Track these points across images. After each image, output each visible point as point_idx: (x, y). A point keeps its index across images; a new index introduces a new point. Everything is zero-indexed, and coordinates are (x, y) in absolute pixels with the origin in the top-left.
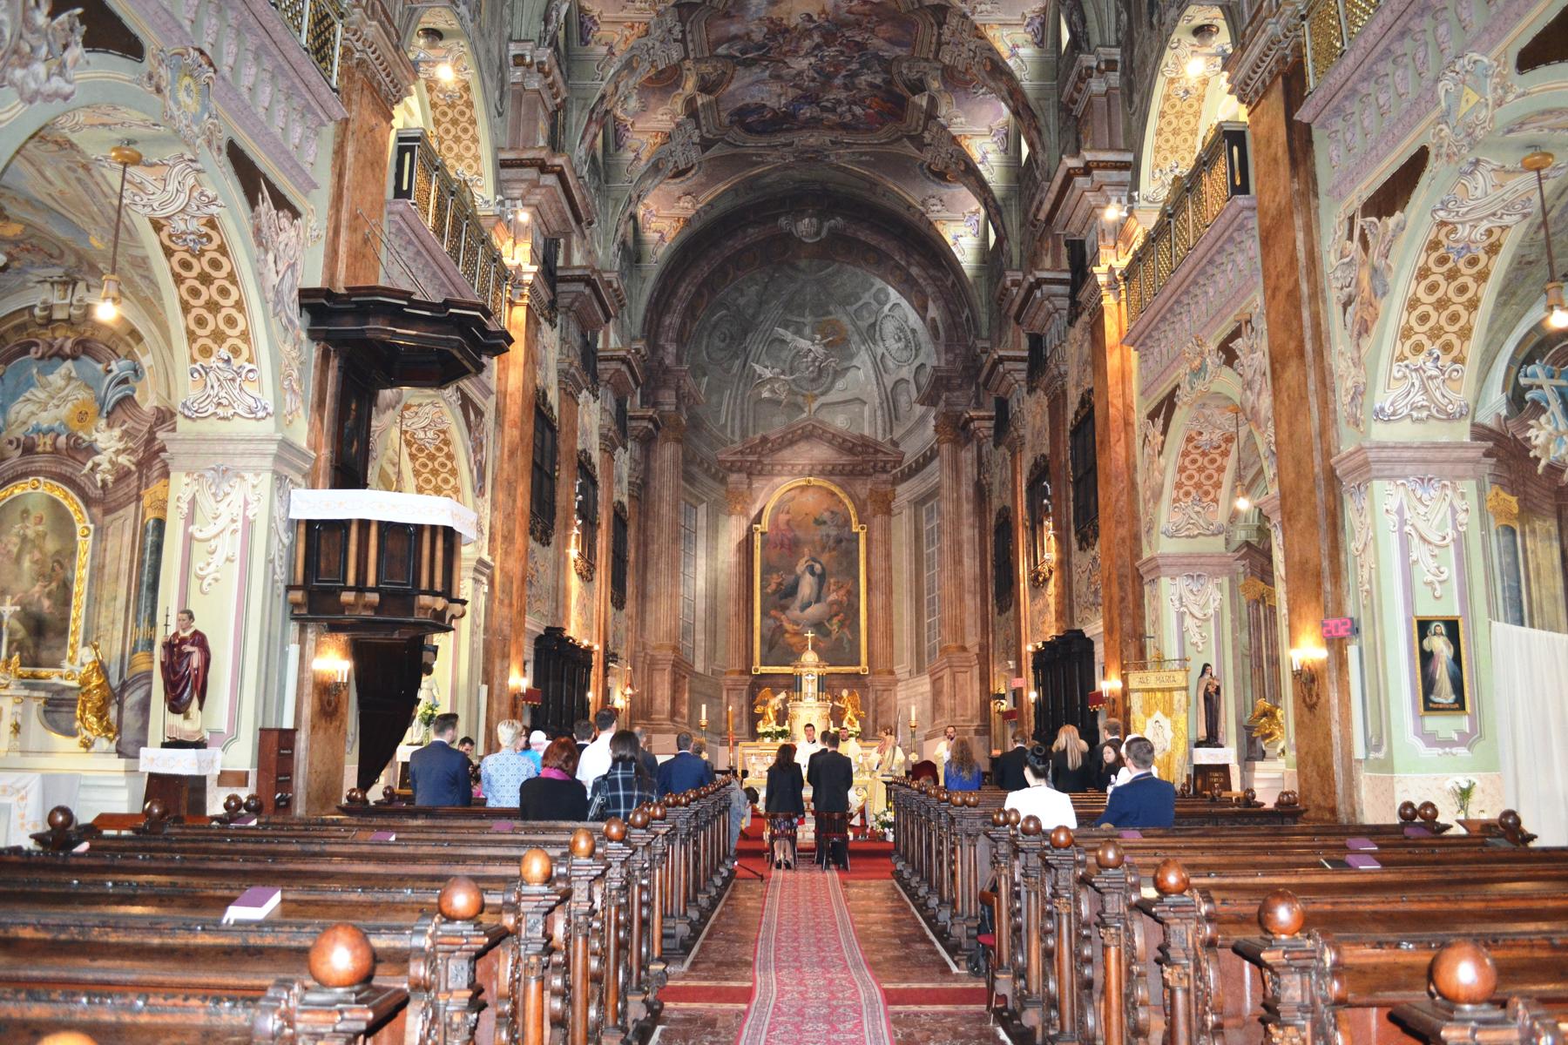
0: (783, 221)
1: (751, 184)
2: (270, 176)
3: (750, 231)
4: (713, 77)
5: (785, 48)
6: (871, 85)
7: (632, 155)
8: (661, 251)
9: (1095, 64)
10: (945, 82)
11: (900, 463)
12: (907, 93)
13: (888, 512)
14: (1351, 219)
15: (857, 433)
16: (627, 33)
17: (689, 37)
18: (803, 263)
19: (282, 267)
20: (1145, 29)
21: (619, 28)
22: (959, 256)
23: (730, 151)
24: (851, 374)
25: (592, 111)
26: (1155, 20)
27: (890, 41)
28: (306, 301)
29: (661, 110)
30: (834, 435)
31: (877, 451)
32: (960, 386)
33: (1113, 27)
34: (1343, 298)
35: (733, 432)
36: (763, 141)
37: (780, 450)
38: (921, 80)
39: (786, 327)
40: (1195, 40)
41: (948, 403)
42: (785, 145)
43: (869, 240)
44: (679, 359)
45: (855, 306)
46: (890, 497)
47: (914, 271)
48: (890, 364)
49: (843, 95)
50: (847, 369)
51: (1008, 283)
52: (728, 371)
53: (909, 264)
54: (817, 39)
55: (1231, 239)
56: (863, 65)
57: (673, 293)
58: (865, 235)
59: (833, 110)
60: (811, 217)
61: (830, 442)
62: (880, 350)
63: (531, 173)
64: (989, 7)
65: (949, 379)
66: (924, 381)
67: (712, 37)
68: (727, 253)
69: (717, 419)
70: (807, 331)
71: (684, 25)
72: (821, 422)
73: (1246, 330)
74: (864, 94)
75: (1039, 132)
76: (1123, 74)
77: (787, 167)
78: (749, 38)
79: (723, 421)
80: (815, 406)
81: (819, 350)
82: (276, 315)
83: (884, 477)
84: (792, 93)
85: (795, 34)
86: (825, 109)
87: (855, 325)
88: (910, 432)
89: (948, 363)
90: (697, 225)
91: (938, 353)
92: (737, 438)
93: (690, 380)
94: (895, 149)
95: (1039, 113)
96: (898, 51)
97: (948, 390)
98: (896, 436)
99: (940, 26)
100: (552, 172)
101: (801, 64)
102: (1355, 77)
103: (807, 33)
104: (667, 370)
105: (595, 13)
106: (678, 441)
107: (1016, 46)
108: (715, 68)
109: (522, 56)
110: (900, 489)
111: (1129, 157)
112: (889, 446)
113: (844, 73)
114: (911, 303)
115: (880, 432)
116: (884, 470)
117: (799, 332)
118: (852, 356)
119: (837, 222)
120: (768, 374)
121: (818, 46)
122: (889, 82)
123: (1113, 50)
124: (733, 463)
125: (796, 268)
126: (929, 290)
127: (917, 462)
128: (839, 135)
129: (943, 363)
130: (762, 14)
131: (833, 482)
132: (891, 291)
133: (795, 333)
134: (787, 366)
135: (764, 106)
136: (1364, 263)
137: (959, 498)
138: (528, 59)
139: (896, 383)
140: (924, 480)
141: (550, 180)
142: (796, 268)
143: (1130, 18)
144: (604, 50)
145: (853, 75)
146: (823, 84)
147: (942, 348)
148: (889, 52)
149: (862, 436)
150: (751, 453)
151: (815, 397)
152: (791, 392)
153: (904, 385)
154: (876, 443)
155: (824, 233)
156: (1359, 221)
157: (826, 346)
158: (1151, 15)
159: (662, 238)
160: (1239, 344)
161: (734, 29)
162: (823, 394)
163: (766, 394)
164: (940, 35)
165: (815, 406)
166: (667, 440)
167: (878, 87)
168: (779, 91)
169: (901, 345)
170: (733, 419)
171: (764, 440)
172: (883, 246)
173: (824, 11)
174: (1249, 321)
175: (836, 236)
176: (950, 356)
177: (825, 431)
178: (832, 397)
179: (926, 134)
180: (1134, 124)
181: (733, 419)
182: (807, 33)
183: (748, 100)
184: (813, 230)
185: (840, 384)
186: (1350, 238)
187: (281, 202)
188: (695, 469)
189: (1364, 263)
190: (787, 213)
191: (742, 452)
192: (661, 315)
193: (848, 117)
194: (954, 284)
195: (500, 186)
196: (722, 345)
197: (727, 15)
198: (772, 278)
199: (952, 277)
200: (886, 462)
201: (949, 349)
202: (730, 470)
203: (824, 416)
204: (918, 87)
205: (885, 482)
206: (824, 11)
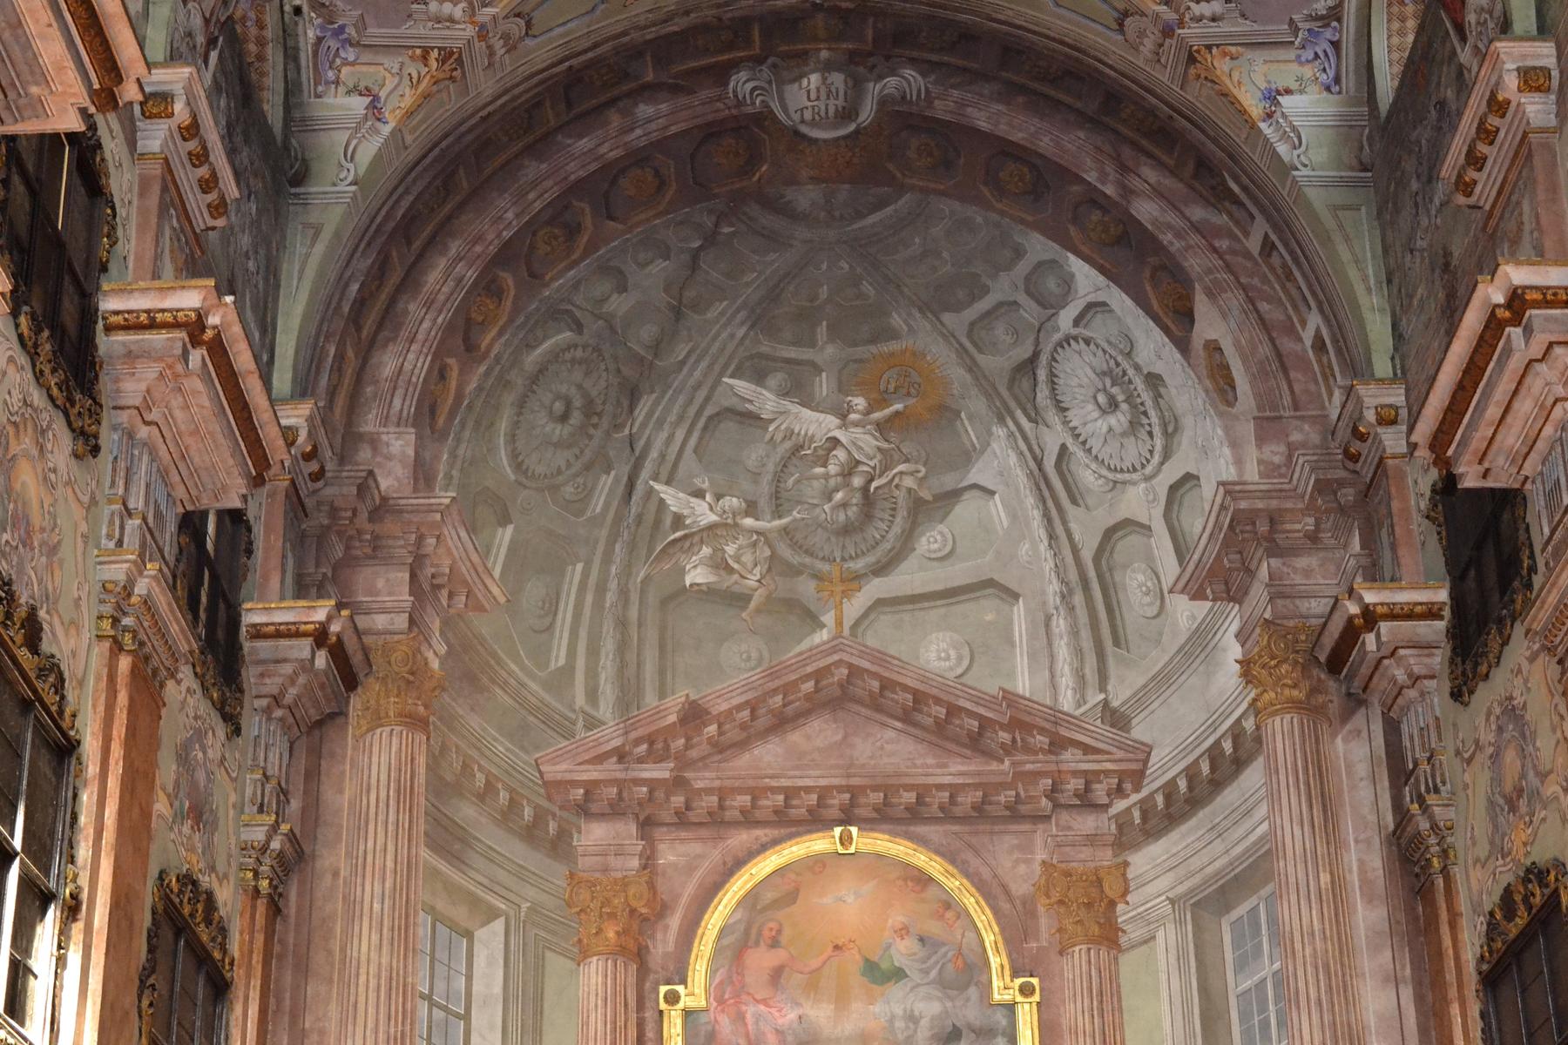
0: (742, 83)
3: (644, 110)
8: (368, 151)
11: (1138, 777)
13: (1109, 936)
15: (991, 687)
18: (806, 197)
22: (1282, 149)
24: (966, 510)
30: (919, 698)
31: (1058, 744)
32: (1313, 538)
35: (593, 695)
37: (743, 745)
39: (759, 378)
41: (1278, 592)
43: (1003, 130)
44: (422, 475)
45: (971, 313)
46: (1111, 888)
47: (1146, 210)
48: (1087, 476)
50: (954, 495)
52: (578, 505)
53: (1127, 192)
57: (410, 281)
60: (828, 67)
61: (907, 717)
62: (1052, 439)
65: (1274, 519)
66: (1197, 521)
68: (575, 171)
69: (541, 654)
70: (824, 386)
72: (881, 657)
79: (559, 658)
80: (854, 607)
81: (863, 441)
83: (1087, 823)
87: (972, 367)
88: (1162, 681)
89: (1268, 470)
91: (1234, 444)
92: (605, 710)
93: (456, 539)
97: (1275, 550)
98: (1119, 694)
104: (383, 508)
106: (417, 723)
110: (1141, 861)
115: (1066, 680)
116: (1086, 802)
117: (798, 390)
118: (967, 458)
119: (907, 81)
120: (703, 513)
124: (591, 788)
126: (1196, 263)
127: (1191, 773)
129: (1252, 473)
131: (922, 842)
133: (784, 394)
134: (765, 487)
137: (1338, 886)
139: (1110, 533)
140: (1217, 831)
147: (1248, 430)
149: (1010, 698)
150: (655, 757)
153: (1134, 540)
154: (1058, 716)
155: (867, 113)
157: (882, 428)
159: (375, 109)
162: (881, 569)
163: (697, 575)
165: (854, 607)
166: (377, 721)
169: (1119, 420)
170: (593, 652)
171: (694, 715)
172: (1045, 145)
176: (1275, 452)
177: (887, 685)
178: (908, 578)
181: (593, 652)
184: (834, 105)
185: (930, 540)
188: (466, 812)
190: (759, 60)
191: (621, 755)
192: (367, 351)
194: (1268, 247)
196: (559, 431)
198: (711, 239)
199: (1260, 228)
200: (1090, 778)
201: (1268, 425)
202: (585, 810)
203: (885, 636)
205: (1092, 840)
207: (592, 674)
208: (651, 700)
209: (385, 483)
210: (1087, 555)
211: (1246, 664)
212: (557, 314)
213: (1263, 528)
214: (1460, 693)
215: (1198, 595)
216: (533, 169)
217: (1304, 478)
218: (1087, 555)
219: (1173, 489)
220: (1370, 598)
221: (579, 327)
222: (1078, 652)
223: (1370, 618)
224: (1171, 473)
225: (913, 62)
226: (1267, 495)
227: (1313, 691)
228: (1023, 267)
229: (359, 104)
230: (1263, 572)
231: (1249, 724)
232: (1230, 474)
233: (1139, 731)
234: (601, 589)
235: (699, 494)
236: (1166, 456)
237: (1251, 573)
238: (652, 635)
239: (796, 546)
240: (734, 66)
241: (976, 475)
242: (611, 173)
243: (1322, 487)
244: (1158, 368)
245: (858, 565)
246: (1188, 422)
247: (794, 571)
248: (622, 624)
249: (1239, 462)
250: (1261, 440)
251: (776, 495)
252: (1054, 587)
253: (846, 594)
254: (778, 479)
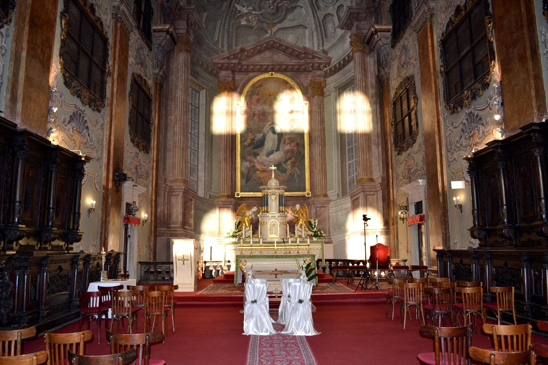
11: (329, 64)
13: (322, 94)
15: (301, 45)
24: (297, 11)
30: (287, 48)
31: (314, 57)
32: (365, 18)
35: (223, 46)
37: (252, 56)
41: (358, 28)
46: (323, 85)
50: (295, 8)
61: (284, 51)
65: (358, 14)
66: (343, 14)
72: (280, 40)
79: (216, 39)
80: (274, 29)
83: (319, 72)
88: (334, 45)
92: (225, 49)
97: (358, 20)
98: (326, 48)
104: (181, 9)
106: (188, 51)
110: (329, 80)
112: (322, 54)
115: (316, 45)
116: (319, 68)
120: (245, 10)
124: (222, 64)
127: (339, 63)
129: (354, 4)
131: (287, 75)
134: (257, 5)
137: (366, 85)
139: (325, 16)
140: (344, 75)
149: (305, 48)
150: (235, 58)
151: (274, 24)
152: (259, 21)
153: (330, 17)
154: (314, 52)
162: (280, 22)
163: (243, 23)
165: (274, 29)
166: (181, 51)
170: (223, 38)
171: (243, 50)
177: (281, 45)
178: (286, 24)
181: (223, 38)
185: (290, 17)
188: (198, 69)
191: (228, 58)
200: (320, 64)
202: (221, 68)
203: (280, 35)
205: (320, 76)
207: (223, 42)
208: (234, 47)
209: (181, 4)
210: (321, 20)
211: (351, 42)
213: (356, 16)
214: (393, 47)
215: (342, 29)
218: (321, 20)
219: (338, 7)
220: (377, 27)
222: (318, 40)
223: (376, 31)
224: (338, 4)
226: (356, 9)
227: (363, 48)
231: (351, 54)
232: (349, 5)
233: (330, 55)
234: (224, 25)
235: (244, 6)
237: (353, 25)
238: (234, 34)
239: (263, 17)
241: (299, 4)
243: (367, 8)
245: (276, 21)
247: (263, 22)
248: (228, 32)
251: (259, 7)
252: (314, 26)
253: (273, 27)
254: (260, 4)
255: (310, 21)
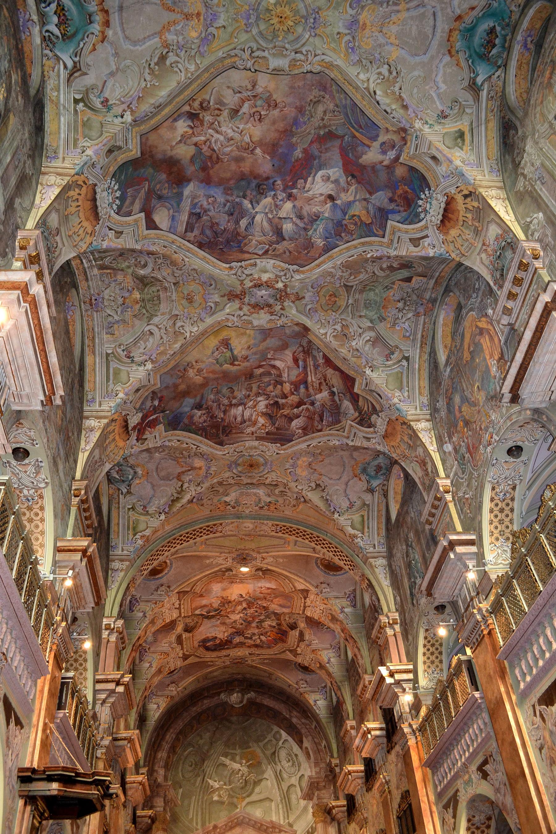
0: (223, 696)
1: (205, 677)
2: (17, 710)
3: (205, 701)
4: (192, 623)
5: (228, 610)
6: (270, 626)
7: (148, 665)
8: (157, 715)
9: (387, 621)
10: (307, 623)
12: (288, 629)
14: (534, 706)
15: (268, 820)
16: (153, 606)
17: (182, 606)
18: (234, 719)
19: (14, 757)
20: (410, 605)
21: (149, 604)
23: (197, 660)
24: (263, 783)
25: (134, 645)
26: (415, 602)
27: (280, 605)
28: (21, 774)
29: (164, 641)
30: (255, 822)
32: (325, 787)
33: (393, 603)
34: (539, 746)
35: (197, 824)
36: (214, 654)
38: (295, 623)
39: (226, 757)
40: (436, 612)
42: (225, 656)
43: (269, 704)
44: (166, 778)
47: (294, 720)
48: (285, 776)
49: (256, 631)
50: (261, 780)
51: (349, 728)
52: (194, 784)
53: (291, 717)
54: (244, 605)
55: (474, 713)
56: (268, 617)
57: (163, 739)
58: (268, 702)
59: (251, 638)
60: (238, 692)
61: (253, 827)
62: (279, 768)
63: (112, 686)
64: (328, 590)
66: (304, 784)
67: (193, 606)
69: (188, 815)
70: (238, 758)
71: (180, 601)
72: (248, 814)
73: (491, 760)
74: (267, 630)
75: (359, 650)
76: (401, 625)
77: (225, 667)
78: (211, 606)
81: (245, 769)
82: (8, 784)
84: (231, 631)
85: (234, 603)
86: (246, 638)
87: (264, 754)
88: (299, 817)
90: (177, 699)
91: (310, 767)
92: (199, 827)
93: (172, 792)
94: (283, 656)
95: (357, 640)
96: (285, 610)
98: (291, 820)
99: (305, 598)
100: (122, 685)
101: (235, 617)
102: (522, 641)
103: (240, 603)
104: (159, 786)
105: (138, 597)
107: (343, 608)
108: (193, 620)
109: (110, 625)
111: (411, 667)
112: (287, 827)
113: (257, 621)
114: (294, 739)
115: (282, 818)
117: (233, 759)
118: (263, 772)
119: (252, 695)
120: (216, 785)
121: (245, 609)
122: (279, 625)
123: (395, 614)
125: (231, 722)
126: (303, 731)
128: (253, 650)
129: (314, 774)
130: (219, 595)
132: (283, 732)
133: (231, 760)
134: (227, 780)
135: (216, 638)
136: (545, 728)
138: (112, 626)
139: (289, 787)
141: (121, 689)
142: (231, 722)
143: (401, 599)
144: (141, 614)
145: (261, 621)
146: (246, 626)
147: (313, 765)
148: (279, 610)
149: (272, 822)
151: (244, 798)
152: (230, 796)
154: (280, 826)
155: (245, 702)
156: (538, 708)
157: (248, 767)
158: (412, 600)
160: (487, 768)
161: (204, 602)
162: (248, 796)
163: (216, 798)
164: (305, 603)
166: (158, 830)
167: (274, 627)
168: (224, 630)
169: (290, 764)
173: (248, 593)
174: (491, 756)
175: (251, 702)
176: (318, 769)
177: (250, 820)
178: (254, 797)
179: (298, 649)
180: (411, 650)
181: (197, 815)
182: (240, 603)
183: (209, 635)
184: (239, 700)
185: (257, 790)
186: (535, 715)
187: (18, 723)
189: (545, 728)
192: (156, 752)
193: (258, 641)
194: (316, 727)
195: (95, 692)
196: (190, 769)
197: (201, 596)
198: (217, 728)
201: (316, 764)
204: (293, 627)
206: (248, 593)
207: (197, 819)
208: (207, 824)
209: (159, 780)
210: (285, 792)
211: (313, 813)
212: (190, 745)
215: (305, 799)
216: (185, 714)
217: (323, 775)
218: (285, 792)
219: (300, 777)
221: (194, 747)
222: (284, 812)
224: (300, 774)
225: (254, 691)
226: (316, 778)
227: (325, 818)
228: (273, 732)
229: (156, 706)
230: (316, 794)
231: (314, 825)
232: (310, 774)
233: (295, 828)
234: (198, 802)
235: (216, 781)
236: (299, 771)
237: (314, 794)
238: (207, 811)
239: (233, 792)
240: (221, 692)
241: (265, 776)
242: (200, 714)
243: (326, 776)
244: (297, 753)
245: (244, 795)
246: (302, 764)
247: (233, 797)
248: (202, 809)
249: (311, 771)
250: (315, 767)
251: (229, 781)
252: (279, 799)
253: (242, 801)
254: (230, 778)
255: (276, 794)
